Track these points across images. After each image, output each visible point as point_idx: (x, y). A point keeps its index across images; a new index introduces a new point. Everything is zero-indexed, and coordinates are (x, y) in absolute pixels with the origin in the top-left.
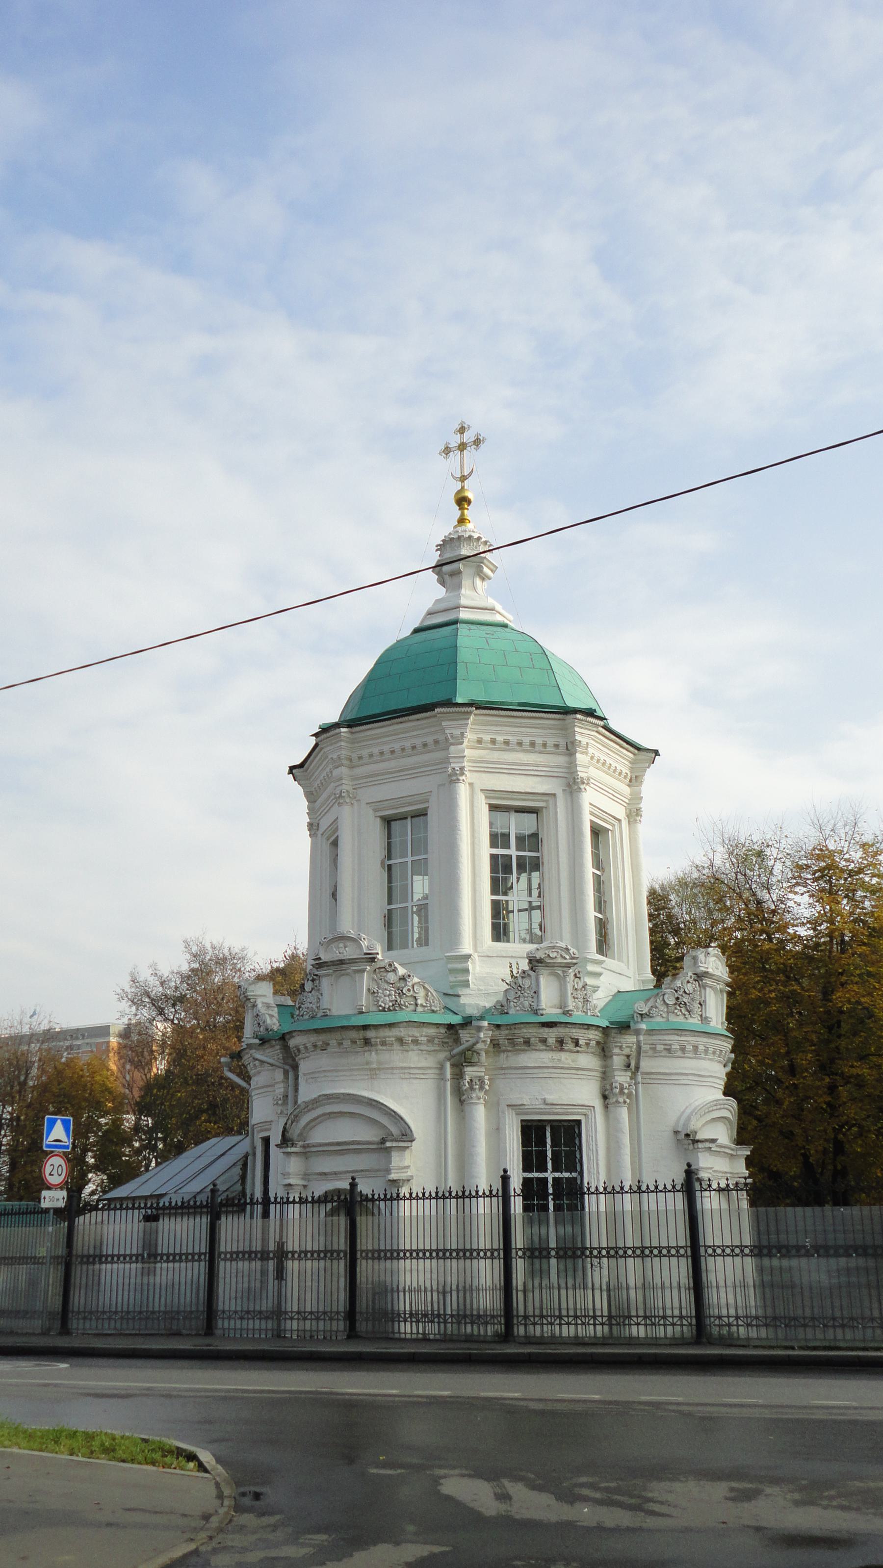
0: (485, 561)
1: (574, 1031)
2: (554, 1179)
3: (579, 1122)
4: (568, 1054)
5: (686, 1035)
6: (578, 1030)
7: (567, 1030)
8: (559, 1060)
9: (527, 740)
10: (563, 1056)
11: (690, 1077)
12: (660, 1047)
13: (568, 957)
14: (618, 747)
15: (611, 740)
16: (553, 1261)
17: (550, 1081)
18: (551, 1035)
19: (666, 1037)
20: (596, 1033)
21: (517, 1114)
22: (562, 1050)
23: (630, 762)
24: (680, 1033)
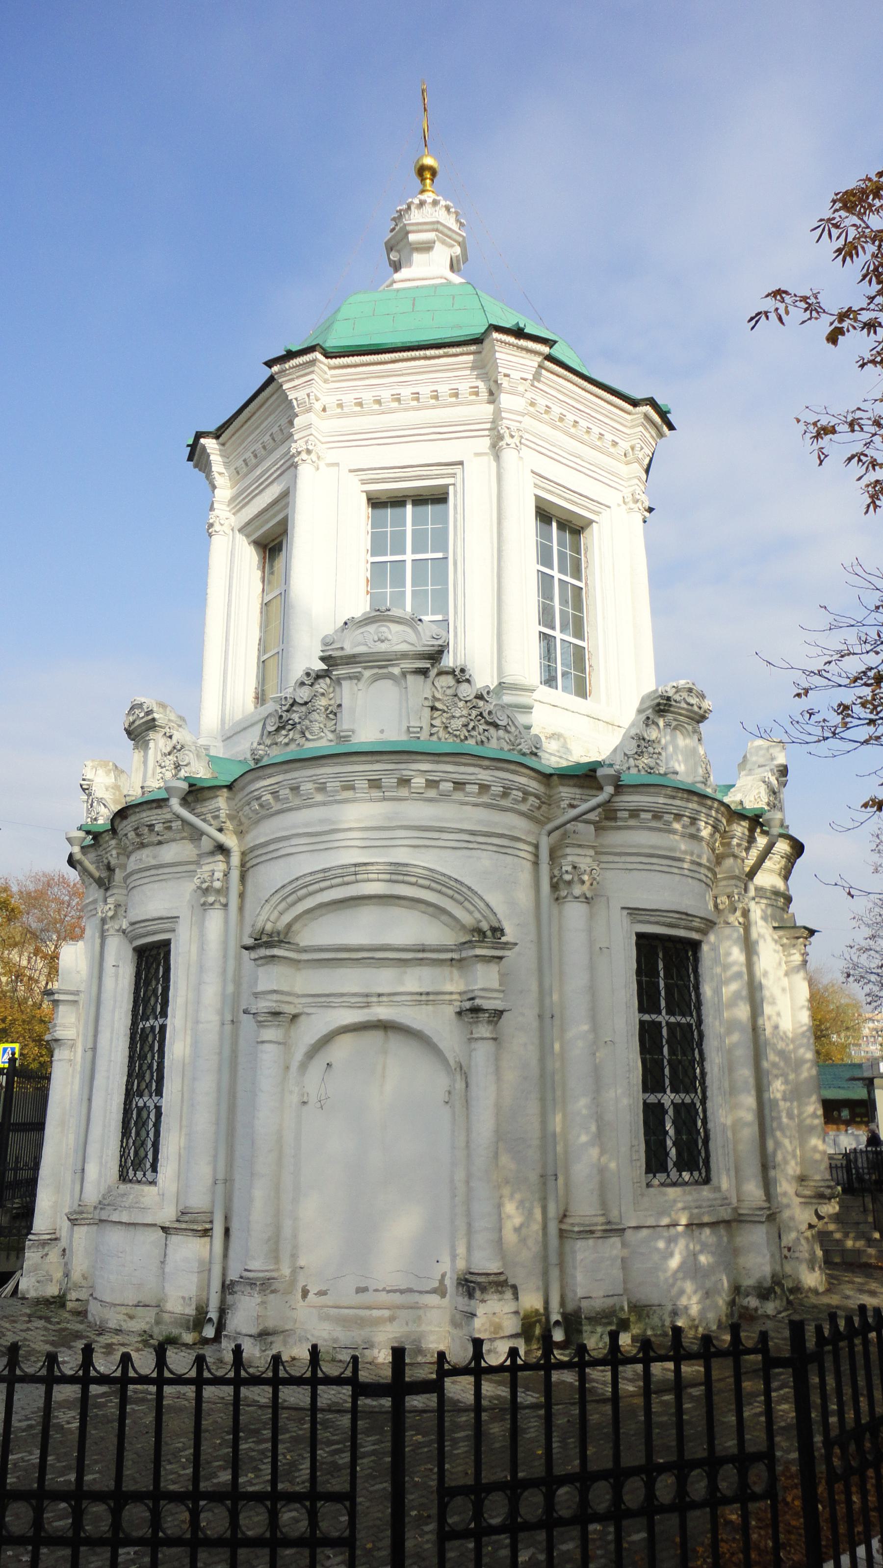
0: (409, 228)
1: (144, 814)
4: (151, 848)
6: (149, 813)
7: (138, 816)
11: (294, 842)
14: (422, 362)
21: (131, 942)
22: (143, 845)
23: (473, 368)
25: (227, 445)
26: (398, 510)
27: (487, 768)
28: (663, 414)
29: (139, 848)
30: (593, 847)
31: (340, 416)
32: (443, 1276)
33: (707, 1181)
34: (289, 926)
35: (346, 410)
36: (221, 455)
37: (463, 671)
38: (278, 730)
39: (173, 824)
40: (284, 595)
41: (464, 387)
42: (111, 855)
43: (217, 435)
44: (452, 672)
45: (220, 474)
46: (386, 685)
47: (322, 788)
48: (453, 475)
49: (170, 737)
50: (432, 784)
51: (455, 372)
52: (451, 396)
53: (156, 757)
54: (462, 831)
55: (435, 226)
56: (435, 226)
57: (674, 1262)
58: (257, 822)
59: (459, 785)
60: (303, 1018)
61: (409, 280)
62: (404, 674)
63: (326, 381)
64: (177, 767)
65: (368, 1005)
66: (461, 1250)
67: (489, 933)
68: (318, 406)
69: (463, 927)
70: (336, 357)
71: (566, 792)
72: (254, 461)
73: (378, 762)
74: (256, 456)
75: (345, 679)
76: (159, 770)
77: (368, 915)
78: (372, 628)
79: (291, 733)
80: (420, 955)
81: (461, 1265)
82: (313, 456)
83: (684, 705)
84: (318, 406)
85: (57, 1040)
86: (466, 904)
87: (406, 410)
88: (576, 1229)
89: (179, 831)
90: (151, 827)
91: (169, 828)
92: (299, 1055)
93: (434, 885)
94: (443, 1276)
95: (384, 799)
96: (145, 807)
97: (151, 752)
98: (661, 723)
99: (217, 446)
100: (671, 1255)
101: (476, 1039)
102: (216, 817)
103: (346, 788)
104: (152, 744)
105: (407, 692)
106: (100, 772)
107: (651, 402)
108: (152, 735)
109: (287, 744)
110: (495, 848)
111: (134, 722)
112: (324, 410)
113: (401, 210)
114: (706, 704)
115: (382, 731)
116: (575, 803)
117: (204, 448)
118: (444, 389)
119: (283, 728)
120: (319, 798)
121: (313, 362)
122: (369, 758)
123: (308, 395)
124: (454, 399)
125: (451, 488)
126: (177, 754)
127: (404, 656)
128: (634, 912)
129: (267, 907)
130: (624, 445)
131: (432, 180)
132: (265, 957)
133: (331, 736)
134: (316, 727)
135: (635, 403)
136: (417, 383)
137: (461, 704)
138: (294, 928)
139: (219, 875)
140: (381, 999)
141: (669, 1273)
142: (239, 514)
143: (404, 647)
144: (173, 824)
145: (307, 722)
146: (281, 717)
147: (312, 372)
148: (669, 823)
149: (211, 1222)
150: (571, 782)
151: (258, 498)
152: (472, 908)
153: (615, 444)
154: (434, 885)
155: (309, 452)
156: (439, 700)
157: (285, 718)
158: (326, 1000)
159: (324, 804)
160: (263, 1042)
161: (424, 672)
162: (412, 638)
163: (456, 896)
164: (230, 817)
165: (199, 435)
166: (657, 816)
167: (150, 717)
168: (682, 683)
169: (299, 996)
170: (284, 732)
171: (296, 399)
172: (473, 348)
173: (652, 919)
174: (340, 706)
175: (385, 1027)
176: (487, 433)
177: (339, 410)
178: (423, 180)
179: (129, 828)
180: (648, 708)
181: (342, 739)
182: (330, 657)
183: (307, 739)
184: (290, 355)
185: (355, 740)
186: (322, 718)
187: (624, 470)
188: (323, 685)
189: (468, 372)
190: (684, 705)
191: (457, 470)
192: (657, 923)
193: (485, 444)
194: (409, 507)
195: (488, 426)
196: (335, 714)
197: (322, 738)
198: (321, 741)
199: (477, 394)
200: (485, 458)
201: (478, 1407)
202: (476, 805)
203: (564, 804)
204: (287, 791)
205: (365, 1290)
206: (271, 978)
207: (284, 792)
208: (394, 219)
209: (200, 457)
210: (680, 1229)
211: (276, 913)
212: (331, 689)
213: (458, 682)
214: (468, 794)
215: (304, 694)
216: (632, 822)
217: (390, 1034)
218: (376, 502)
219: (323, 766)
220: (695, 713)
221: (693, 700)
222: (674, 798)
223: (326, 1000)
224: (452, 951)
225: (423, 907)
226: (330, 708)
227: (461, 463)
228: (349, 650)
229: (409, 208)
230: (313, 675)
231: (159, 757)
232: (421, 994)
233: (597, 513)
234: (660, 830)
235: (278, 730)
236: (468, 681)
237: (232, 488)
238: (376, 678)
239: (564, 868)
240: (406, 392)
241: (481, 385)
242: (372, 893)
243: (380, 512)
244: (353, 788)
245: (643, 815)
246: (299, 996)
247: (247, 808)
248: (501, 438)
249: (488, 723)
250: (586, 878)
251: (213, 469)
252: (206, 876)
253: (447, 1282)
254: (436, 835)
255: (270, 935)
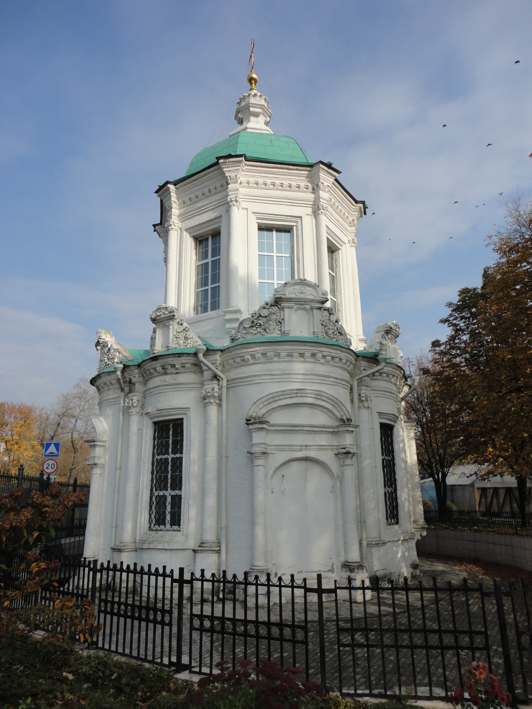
0: (250, 105)
1: (170, 359)
2: (172, 458)
3: (182, 419)
4: (171, 375)
5: (321, 347)
6: (172, 359)
7: (165, 360)
8: (165, 380)
9: (206, 190)
10: (167, 377)
11: (262, 377)
12: (337, 360)
13: (167, 313)
14: (286, 171)
15: (274, 168)
16: (477, 509)
17: (159, 394)
18: (157, 365)
19: (239, 352)
20: (189, 358)
21: (151, 419)
22: (166, 374)
23: (307, 177)
24: (246, 346)
25: (179, 189)
26: (269, 233)
27: (343, 352)
28: (365, 208)
29: (162, 375)
30: (370, 387)
31: (247, 187)
32: (333, 564)
33: (397, 523)
34: (264, 414)
35: (250, 185)
36: (176, 194)
37: (332, 309)
38: (252, 327)
39: (186, 365)
40: (216, 264)
41: (302, 184)
42: (135, 377)
43: (175, 184)
44: (328, 310)
45: (174, 202)
46: (300, 312)
47: (278, 355)
48: (297, 222)
49: (182, 324)
50: (324, 357)
51: (299, 178)
52: (297, 187)
53: (173, 331)
54: (334, 377)
55: (262, 107)
56: (261, 107)
57: (399, 555)
58: (237, 367)
59: (333, 358)
60: (270, 455)
61: (253, 129)
62: (312, 309)
63: (243, 171)
64: (186, 338)
65: (301, 450)
66: (343, 553)
67: (346, 421)
68: (239, 181)
69: (337, 418)
70: (249, 161)
71: (363, 363)
72: (196, 200)
73: (304, 345)
74: (197, 197)
75: (286, 308)
76: (175, 339)
77: (305, 411)
78: (298, 287)
79: (259, 329)
80: (322, 429)
81: (342, 559)
82: (238, 203)
83: (394, 331)
84: (239, 181)
85: (95, 464)
86: (338, 408)
87: (277, 190)
88: (373, 543)
89: (190, 368)
90: (173, 366)
91: (184, 367)
92: (271, 472)
93: (327, 400)
94: (333, 564)
95: (305, 362)
96: (171, 356)
97: (171, 331)
98: (387, 338)
99: (174, 189)
100: (398, 552)
101: (347, 465)
102: (216, 363)
103: (288, 356)
104: (171, 327)
105: (313, 317)
106: (108, 336)
107: (363, 203)
108: (171, 322)
109: (255, 334)
110: (341, 385)
111: (160, 315)
112: (241, 183)
113: (244, 96)
114: (400, 331)
115: (301, 332)
116: (366, 368)
117: (169, 189)
118: (294, 184)
119: (253, 326)
120: (276, 359)
121: (241, 162)
122: (301, 344)
123: (236, 176)
124: (297, 189)
125: (295, 227)
126: (186, 333)
127: (312, 301)
128: (380, 414)
129: (255, 406)
130: (351, 219)
131: (255, 84)
132: (259, 428)
133: (278, 332)
134: (272, 328)
135: (357, 202)
136: (283, 179)
137: (331, 323)
138: (265, 416)
139: (216, 390)
140: (307, 447)
141: (398, 559)
142: (184, 222)
143: (311, 297)
144: (186, 365)
145: (267, 325)
146: (253, 322)
147: (239, 166)
148: (390, 379)
149: (220, 546)
150: (366, 360)
151: (198, 216)
152: (340, 410)
153: (348, 217)
154: (327, 400)
155: (236, 201)
156: (323, 321)
157: (255, 322)
158: (281, 448)
159: (278, 362)
160: (258, 466)
161: (320, 309)
162: (315, 294)
163: (335, 405)
164: (220, 364)
165: (167, 183)
166: (388, 376)
167: (172, 314)
168: (394, 322)
169: (269, 446)
170: (254, 328)
171: (230, 176)
172: (308, 169)
173: (386, 417)
174: (283, 319)
175: (306, 459)
176: (311, 206)
177: (247, 185)
178: (251, 84)
179: (158, 365)
180: (382, 331)
181: (283, 333)
182: (280, 298)
183: (267, 332)
184: (230, 156)
185: (291, 335)
186: (275, 324)
187: (349, 229)
188: (275, 309)
189: (305, 179)
190: (394, 331)
191: (299, 220)
192: (387, 419)
193: (309, 211)
194: (274, 232)
195: (312, 203)
196: (281, 323)
197: (274, 332)
198: (275, 335)
199: (307, 188)
200: (310, 217)
201: (380, 616)
202: (337, 367)
203: (362, 368)
204: (260, 355)
205: (301, 572)
206: (258, 438)
207: (258, 355)
208: (240, 99)
209: (164, 192)
210: (400, 541)
211: (258, 409)
212: (278, 312)
213: (330, 314)
214: (335, 362)
215: (265, 312)
216: (379, 377)
217: (308, 463)
218: (262, 228)
219: (279, 345)
220: (396, 334)
221: (398, 330)
222: (394, 368)
223: (281, 448)
224: (334, 428)
225: (322, 409)
226: (278, 320)
227: (301, 217)
228: (288, 295)
229: (249, 95)
230: (269, 304)
231: (175, 334)
232: (322, 446)
233: (341, 246)
234: (387, 381)
235: (252, 327)
236: (333, 314)
237: (179, 209)
238: (298, 309)
239: (362, 395)
240: (278, 182)
241: (310, 185)
242: (310, 402)
243: (262, 232)
244: (292, 356)
245: (384, 375)
246: (269, 446)
247: (232, 360)
248: (319, 209)
249: (339, 333)
250: (369, 399)
251: (172, 199)
252: (210, 390)
253: (334, 567)
254: (324, 379)
255: (255, 419)
